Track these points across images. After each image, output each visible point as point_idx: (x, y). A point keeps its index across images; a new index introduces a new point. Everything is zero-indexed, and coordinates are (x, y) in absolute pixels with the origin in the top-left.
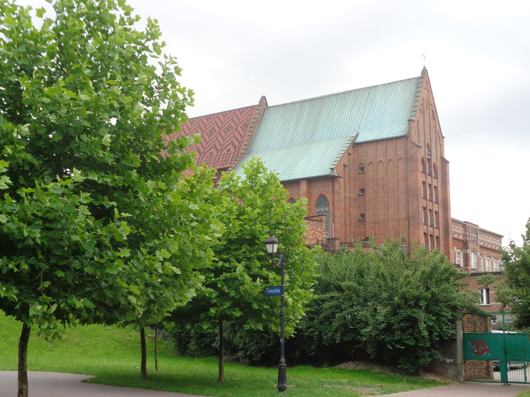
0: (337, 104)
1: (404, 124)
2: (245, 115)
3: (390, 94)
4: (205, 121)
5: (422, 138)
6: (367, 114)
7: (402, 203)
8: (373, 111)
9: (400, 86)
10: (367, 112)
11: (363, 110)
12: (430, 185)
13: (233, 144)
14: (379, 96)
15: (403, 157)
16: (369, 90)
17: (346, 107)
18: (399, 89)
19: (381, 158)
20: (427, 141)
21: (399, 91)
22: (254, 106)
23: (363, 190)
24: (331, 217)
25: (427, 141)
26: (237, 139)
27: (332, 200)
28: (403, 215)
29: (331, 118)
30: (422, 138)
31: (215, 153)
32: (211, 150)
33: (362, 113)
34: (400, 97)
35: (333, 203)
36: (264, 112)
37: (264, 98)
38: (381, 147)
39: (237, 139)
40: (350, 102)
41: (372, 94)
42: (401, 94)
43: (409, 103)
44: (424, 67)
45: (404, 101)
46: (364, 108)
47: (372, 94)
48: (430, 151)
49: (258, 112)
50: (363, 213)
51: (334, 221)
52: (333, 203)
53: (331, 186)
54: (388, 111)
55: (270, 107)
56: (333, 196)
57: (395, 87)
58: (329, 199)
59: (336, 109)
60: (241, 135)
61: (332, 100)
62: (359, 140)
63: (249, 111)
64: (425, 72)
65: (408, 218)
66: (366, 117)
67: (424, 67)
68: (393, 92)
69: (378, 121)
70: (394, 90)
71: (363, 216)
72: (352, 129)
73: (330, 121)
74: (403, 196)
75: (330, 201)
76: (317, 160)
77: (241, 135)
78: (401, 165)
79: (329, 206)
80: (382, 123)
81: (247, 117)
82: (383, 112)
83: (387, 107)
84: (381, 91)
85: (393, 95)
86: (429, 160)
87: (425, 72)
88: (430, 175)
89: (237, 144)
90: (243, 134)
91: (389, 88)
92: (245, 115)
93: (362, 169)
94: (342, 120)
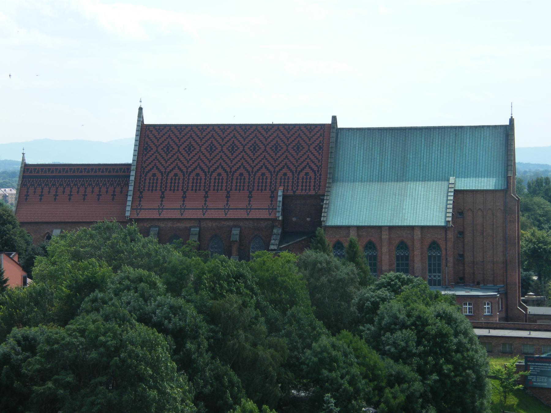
0: (423, 140)
1: (500, 176)
3: (479, 140)
6: (458, 158)
8: (464, 156)
9: (488, 133)
10: (459, 155)
11: (453, 153)
14: (468, 140)
15: (502, 208)
16: (454, 130)
17: (434, 145)
18: (488, 135)
21: (488, 138)
24: (444, 261)
27: (444, 246)
29: (419, 156)
33: (453, 155)
34: (490, 145)
35: (446, 250)
37: (334, 118)
40: (437, 141)
41: (460, 136)
42: (490, 142)
43: (501, 153)
44: (512, 117)
45: (496, 150)
46: (453, 150)
47: (460, 136)
50: (462, 253)
51: (446, 266)
52: (446, 250)
53: (444, 234)
54: (481, 158)
56: (446, 243)
57: (482, 132)
58: (441, 246)
59: (423, 146)
61: (415, 133)
63: (319, 130)
64: (512, 120)
65: (505, 262)
66: (458, 161)
67: (512, 117)
68: (482, 138)
69: (472, 168)
70: (482, 135)
71: (462, 256)
72: (447, 172)
73: (419, 158)
74: (501, 243)
76: (424, 206)
77: (317, 159)
79: (441, 251)
80: (478, 171)
82: (475, 158)
83: (478, 154)
84: (468, 134)
85: (482, 141)
87: (512, 120)
89: (316, 169)
91: (477, 133)
94: (433, 160)
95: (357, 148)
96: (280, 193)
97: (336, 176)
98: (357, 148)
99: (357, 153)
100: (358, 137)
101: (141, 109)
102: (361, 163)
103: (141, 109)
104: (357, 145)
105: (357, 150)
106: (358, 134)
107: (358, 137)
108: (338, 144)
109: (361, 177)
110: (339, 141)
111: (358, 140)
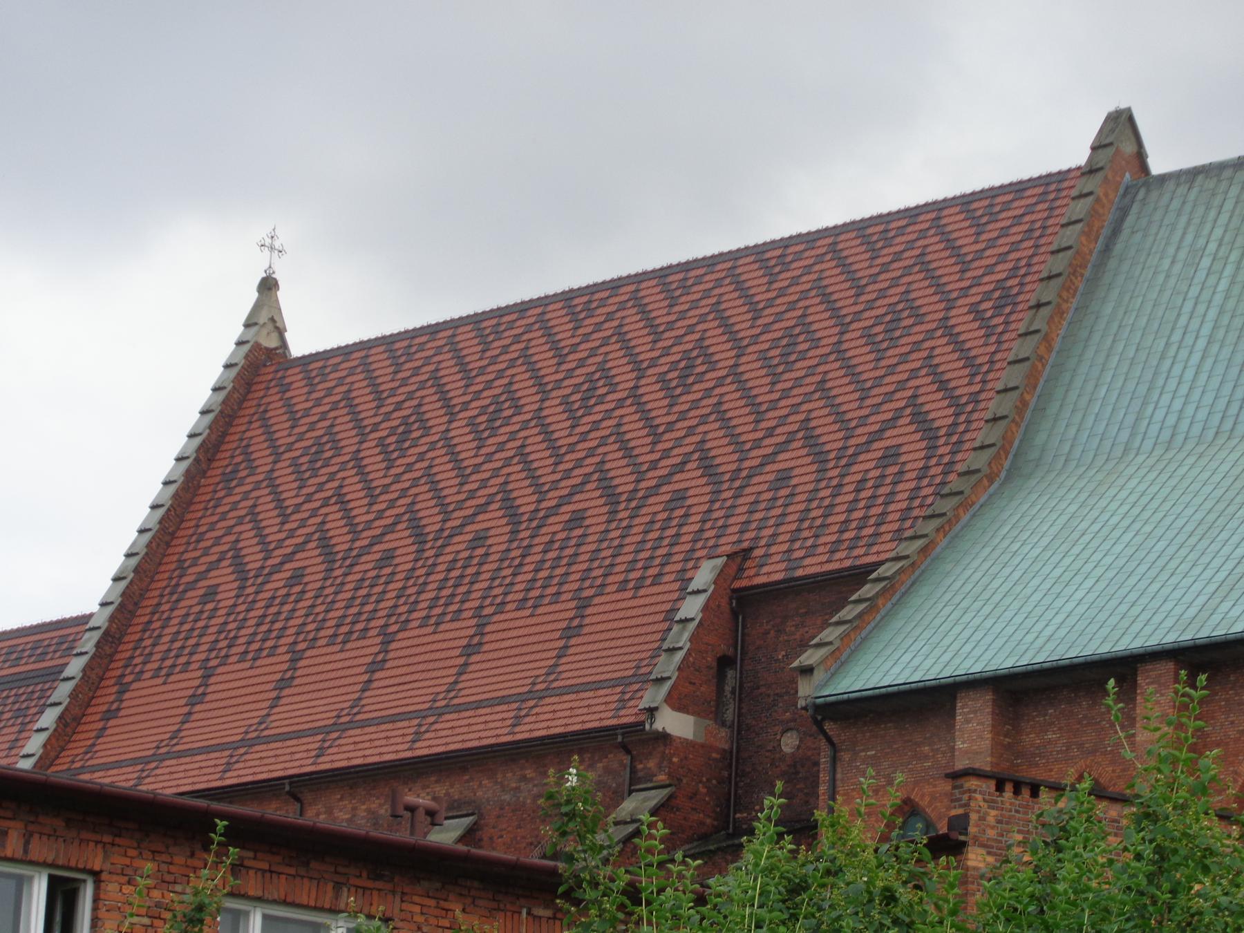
2: (1004, 232)
4: (754, 278)
13: (921, 420)
22: (1062, 176)
26: (943, 385)
31: (804, 476)
32: (784, 460)
36: (1124, 212)
37: (1121, 124)
39: (943, 385)
49: (1080, 208)
55: (1163, 178)
60: (970, 362)
77: (970, 362)
81: (1015, 247)
89: (941, 414)
90: (981, 353)
92: (1004, 232)
95: (1206, 262)
96: (704, 576)
97: (1040, 438)
98: (1206, 262)
99: (1194, 291)
100: (1229, 205)
101: (268, 286)
102: (1201, 343)
103: (268, 286)
104: (1212, 246)
105: (1201, 275)
106: (1234, 191)
107: (1229, 205)
108: (1112, 264)
109: (1171, 420)
110: (1119, 247)
111: (1224, 218)
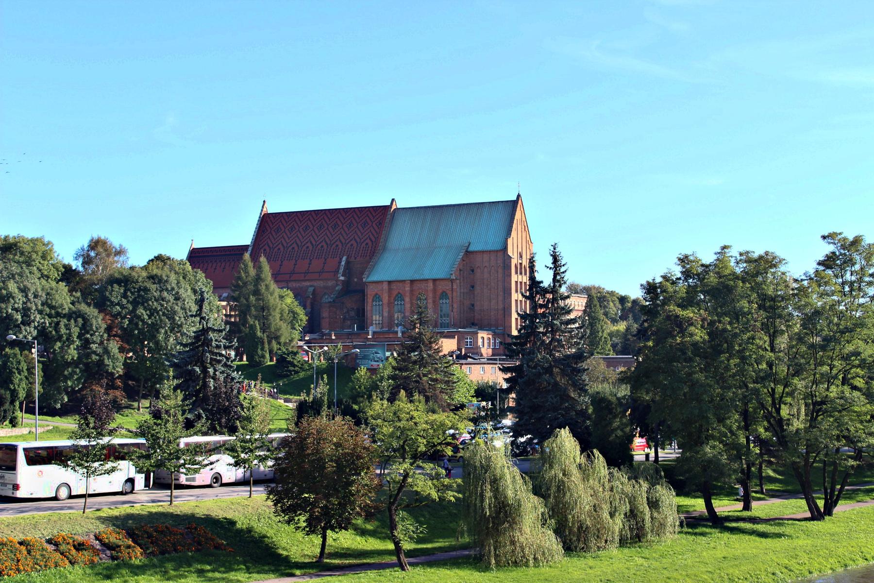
5: (515, 250)
7: (501, 298)
12: (521, 283)
19: (487, 264)
20: (520, 250)
23: (473, 287)
25: (520, 250)
28: (501, 306)
30: (515, 250)
38: (486, 256)
48: (521, 257)
62: (471, 249)
64: (519, 196)
71: (473, 305)
75: (450, 295)
78: (500, 271)
86: (521, 264)
88: (521, 273)
93: (473, 271)
96: (344, 258)
